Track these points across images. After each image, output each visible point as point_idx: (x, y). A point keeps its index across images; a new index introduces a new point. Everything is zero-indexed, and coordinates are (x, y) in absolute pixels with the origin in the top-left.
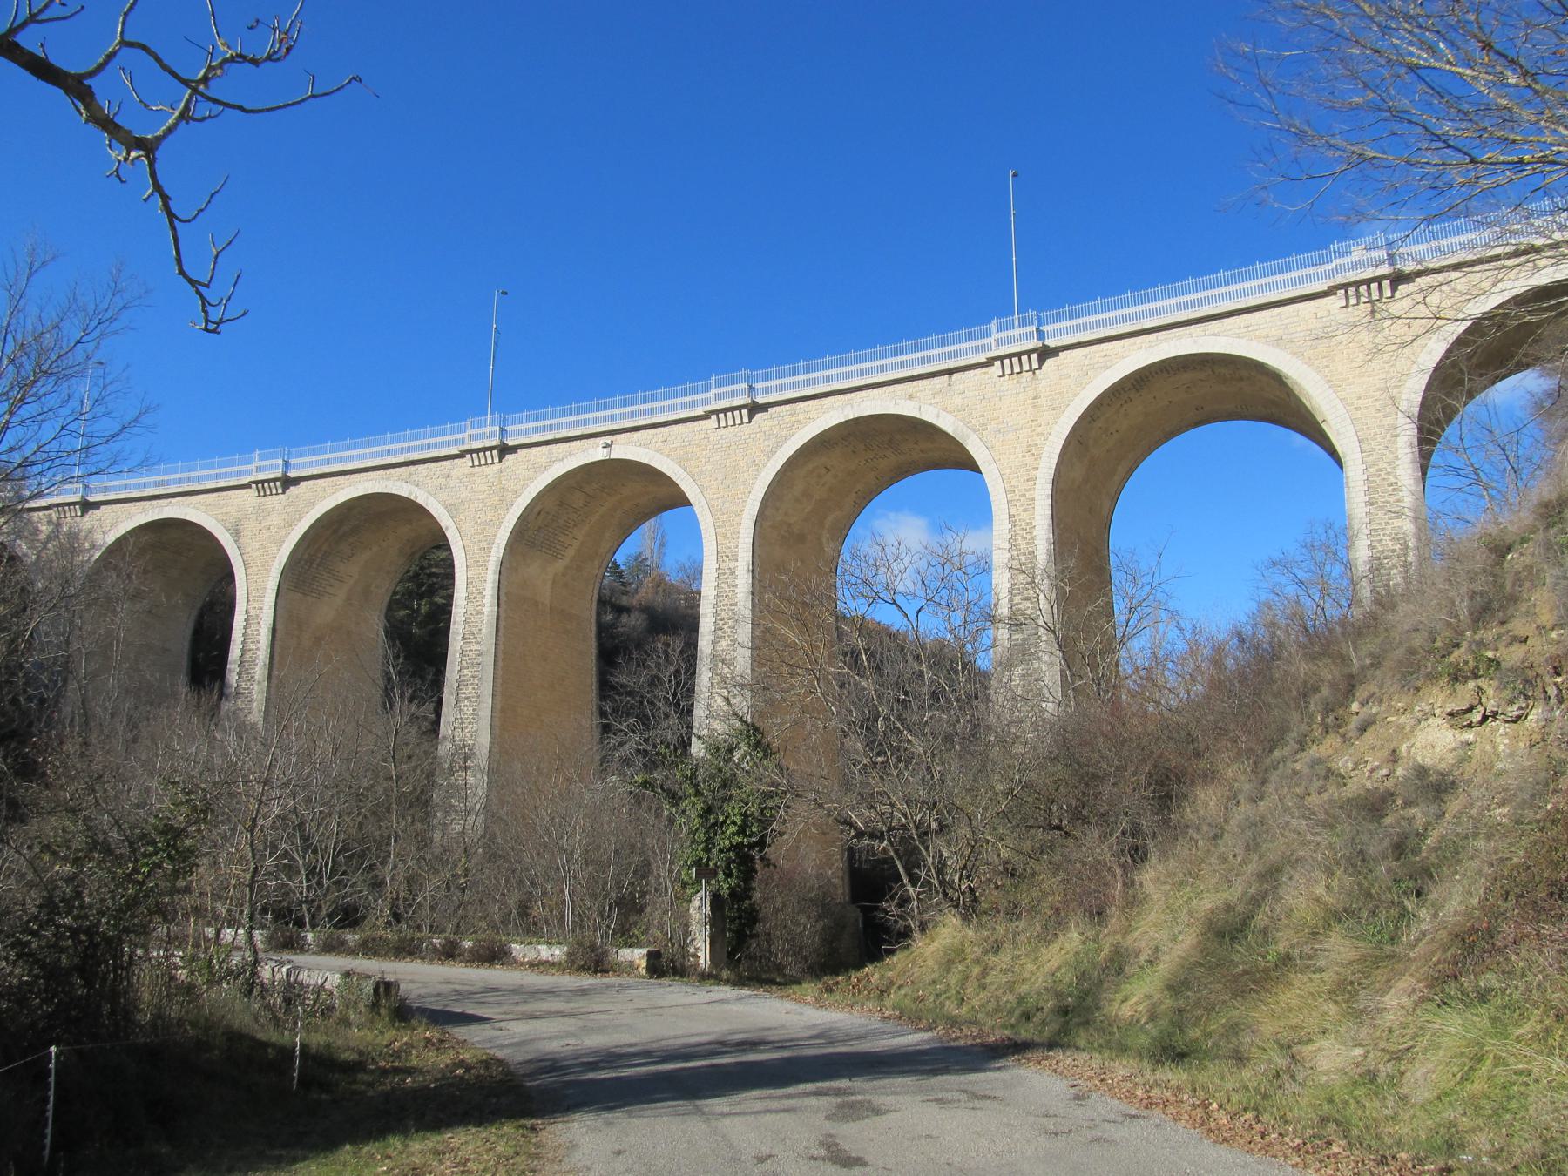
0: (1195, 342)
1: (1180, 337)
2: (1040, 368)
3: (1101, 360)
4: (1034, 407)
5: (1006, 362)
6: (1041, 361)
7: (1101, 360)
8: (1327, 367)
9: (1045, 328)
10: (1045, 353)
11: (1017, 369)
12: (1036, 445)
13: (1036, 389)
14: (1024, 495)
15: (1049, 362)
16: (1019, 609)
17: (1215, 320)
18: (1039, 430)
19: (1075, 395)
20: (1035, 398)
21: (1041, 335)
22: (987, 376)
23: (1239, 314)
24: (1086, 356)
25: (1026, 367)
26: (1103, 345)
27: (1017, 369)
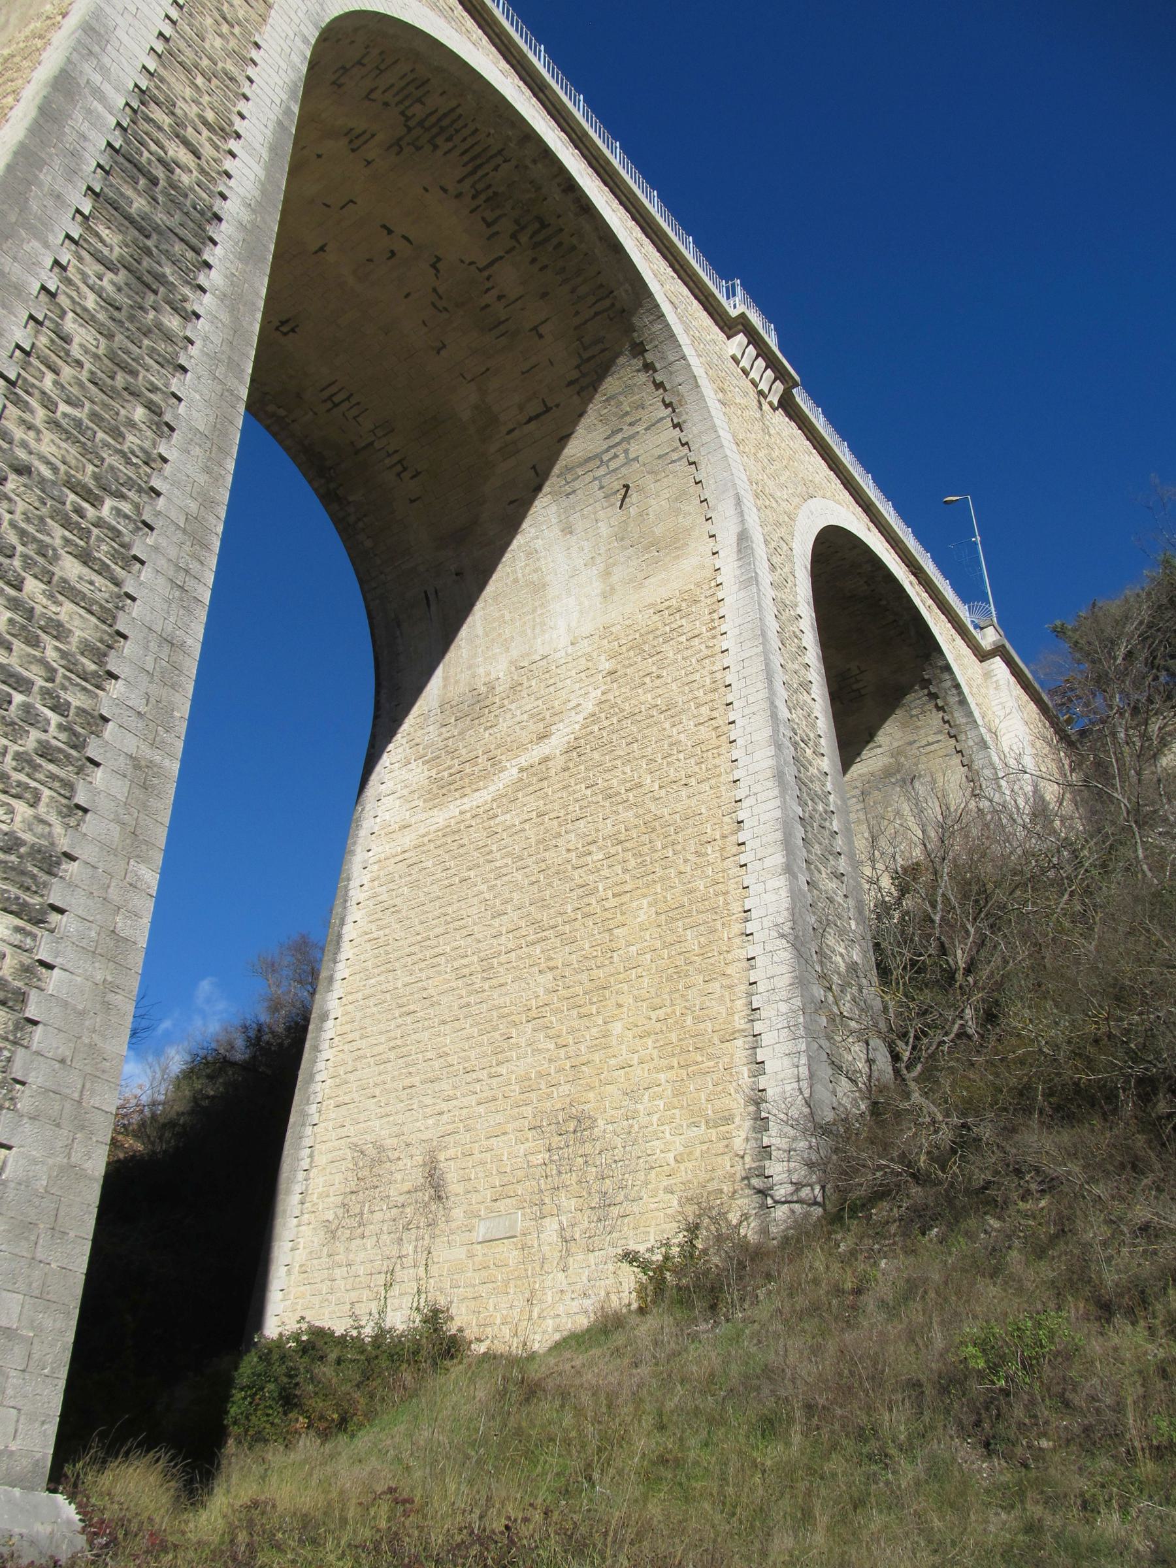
0: (580, 173)
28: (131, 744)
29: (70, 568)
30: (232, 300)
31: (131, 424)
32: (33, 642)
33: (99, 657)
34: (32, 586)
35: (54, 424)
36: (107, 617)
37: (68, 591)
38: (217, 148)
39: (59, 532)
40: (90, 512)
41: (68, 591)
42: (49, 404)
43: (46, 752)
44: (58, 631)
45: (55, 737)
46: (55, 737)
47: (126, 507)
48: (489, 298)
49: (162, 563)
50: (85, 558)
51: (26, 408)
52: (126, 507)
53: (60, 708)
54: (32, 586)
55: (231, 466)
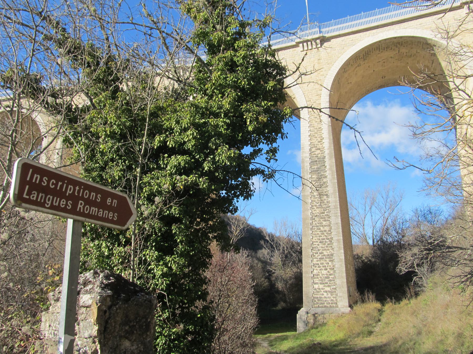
1: (388, 30)
2: (321, 47)
3: (350, 42)
4: (319, 63)
5: (305, 44)
6: (322, 44)
7: (350, 42)
8: (462, 39)
9: (323, 30)
10: (324, 40)
11: (310, 48)
12: (320, 80)
13: (319, 56)
14: (314, 102)
15: (326, 44)
16: (315, 154)
17: (405, 22)
18: (322, 73)
19: (339, 58)
20: (319, 60)
21: (320, 32)
22: (295, 52)
23: (416, 19)
24: (343, 40)
25: (314, 47)
26: (350, 36)
27: (310, 48)
28: (336, 238)
29: (324, 223)
30: (330, 169)
31: (325, 200)
32: (323, 234)
33: (330, 231)
34: (321, 228)
35: (317, 208)
36: (329, 225)
37: (325, 226)
38: (321, 144)
39: (321, 220)
40: (324, 215)
41: (325, 226)
42: (316, 206)
43: (328, 244)
44: (325, 231)
45: (329, 243)
46: (329, 243)
47: (327, 211)
48: (405, 54)
49: (333, 215)
50: (325, 221)
51: (314, 208)
52: (327, 211)
53: (328, 239)
54: (321, 228)
55: (337, 194)
